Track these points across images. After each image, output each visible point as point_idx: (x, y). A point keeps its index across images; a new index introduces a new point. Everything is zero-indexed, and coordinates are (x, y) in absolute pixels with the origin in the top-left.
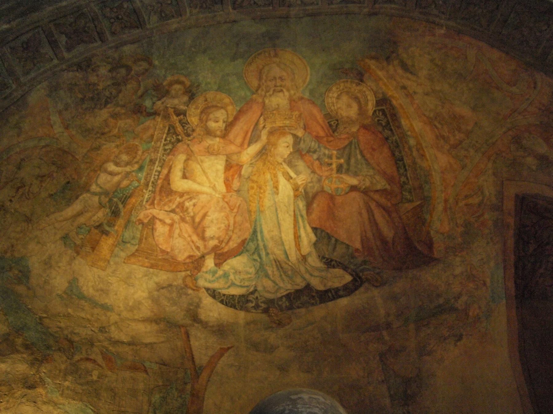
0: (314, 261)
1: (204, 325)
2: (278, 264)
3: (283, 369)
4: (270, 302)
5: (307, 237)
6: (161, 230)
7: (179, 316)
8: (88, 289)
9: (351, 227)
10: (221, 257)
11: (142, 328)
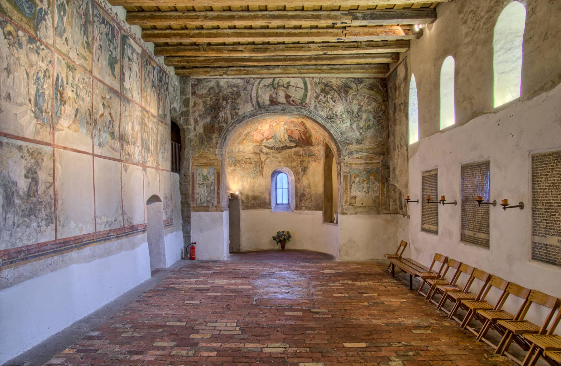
0: (288, 141)
1: (263, 153)
2: (280, 141)
3: (280, 162)
4: (278, 148)
5: (286, 136)
6: (255, 136)
7: (258, 151)
8: (241, 150)
9: (296, 136)
10: (267, 139)
11: (251, 155)
